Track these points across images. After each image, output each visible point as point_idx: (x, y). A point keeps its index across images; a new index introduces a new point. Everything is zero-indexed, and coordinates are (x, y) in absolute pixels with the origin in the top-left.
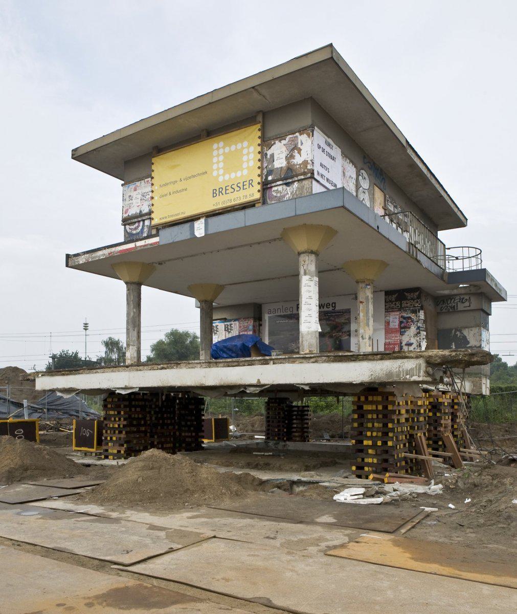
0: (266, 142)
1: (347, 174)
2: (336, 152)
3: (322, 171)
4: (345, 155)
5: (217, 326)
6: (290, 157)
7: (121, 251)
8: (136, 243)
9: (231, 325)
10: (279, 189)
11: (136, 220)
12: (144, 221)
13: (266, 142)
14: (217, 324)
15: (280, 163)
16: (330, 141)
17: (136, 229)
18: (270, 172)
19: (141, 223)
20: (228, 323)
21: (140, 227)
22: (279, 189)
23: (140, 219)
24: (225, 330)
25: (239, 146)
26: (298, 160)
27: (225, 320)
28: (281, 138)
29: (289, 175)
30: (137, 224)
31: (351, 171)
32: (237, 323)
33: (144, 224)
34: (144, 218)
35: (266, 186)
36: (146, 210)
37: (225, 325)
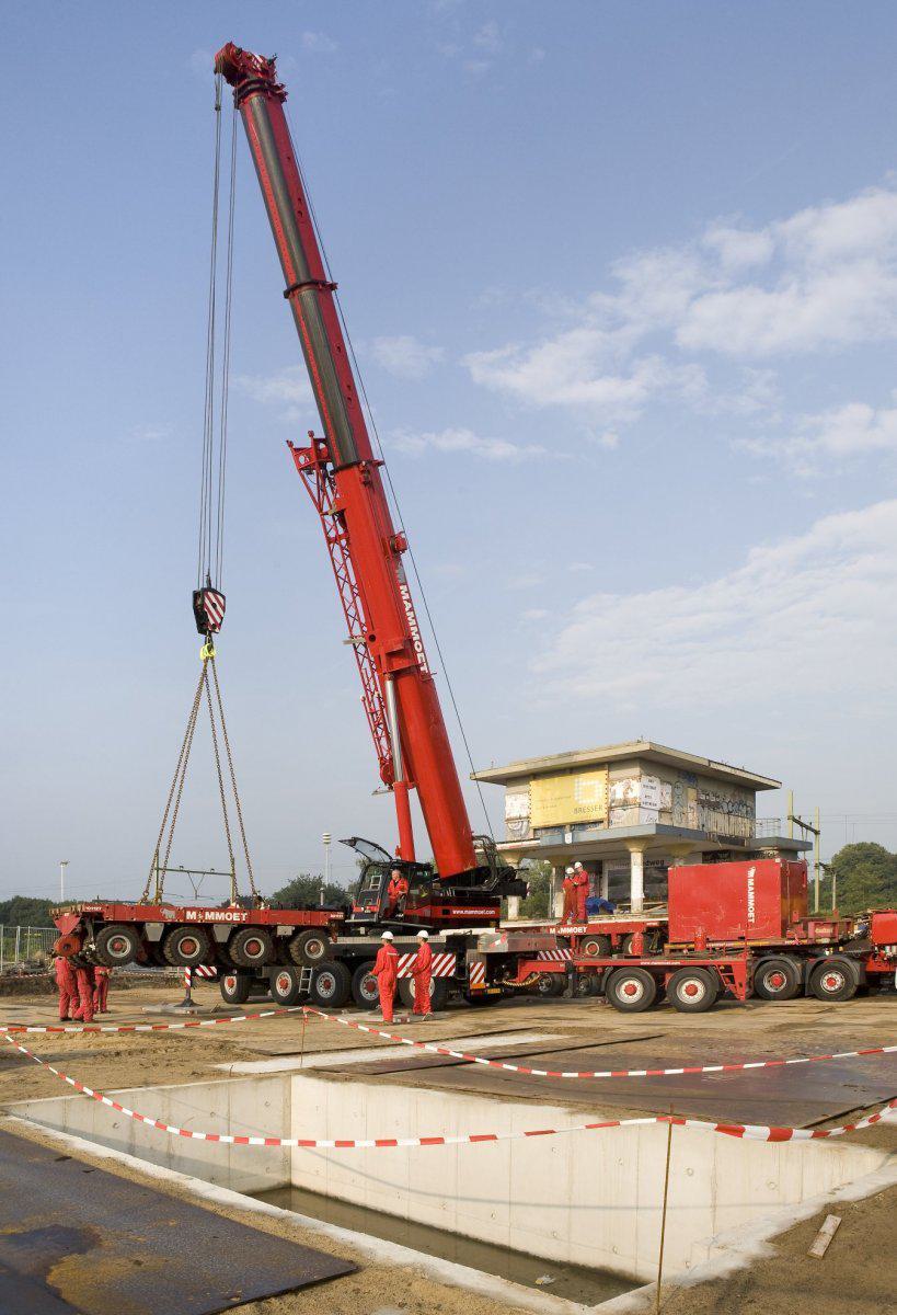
0: (610, 781)
1: (664, 793)
2: (656, 782)
3: (648, 800)
4: (662, 782)
6: (626, 793)
10: (619, 811)
13: (610, 781)
15: (619, 796)
16: (652, 778)
18: (613, 801)
19: (525, 823)
22: (619, 811)
25: (592, 782)
26: (631, 795)
28: (620, 780)
29: (625, 804)
31: (668, 788)
35: (610, 809)
36: (524, 815)
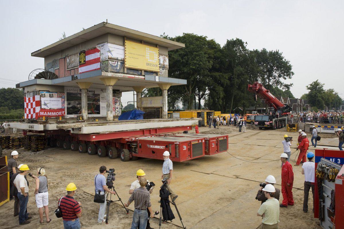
5: (44, 94)
7: (129, 77)
8: (135, 76)
9: (52, 94)
11: (115, 61)
12: (118, 62)
14: (45, 93)
17: (114, 64)
19: (117, 62)
20: (51, 94)
21: (116, 64)
23: (117, 61)
24: (50, 96)
27: (48, 91)
30: (114, 62)
32: (56, 94)
33: (118, 63)
34: (119, 61)
37: (49, 94)
